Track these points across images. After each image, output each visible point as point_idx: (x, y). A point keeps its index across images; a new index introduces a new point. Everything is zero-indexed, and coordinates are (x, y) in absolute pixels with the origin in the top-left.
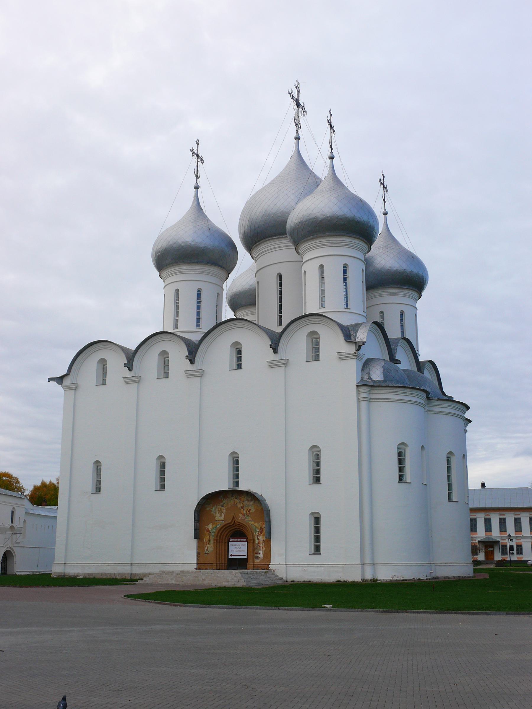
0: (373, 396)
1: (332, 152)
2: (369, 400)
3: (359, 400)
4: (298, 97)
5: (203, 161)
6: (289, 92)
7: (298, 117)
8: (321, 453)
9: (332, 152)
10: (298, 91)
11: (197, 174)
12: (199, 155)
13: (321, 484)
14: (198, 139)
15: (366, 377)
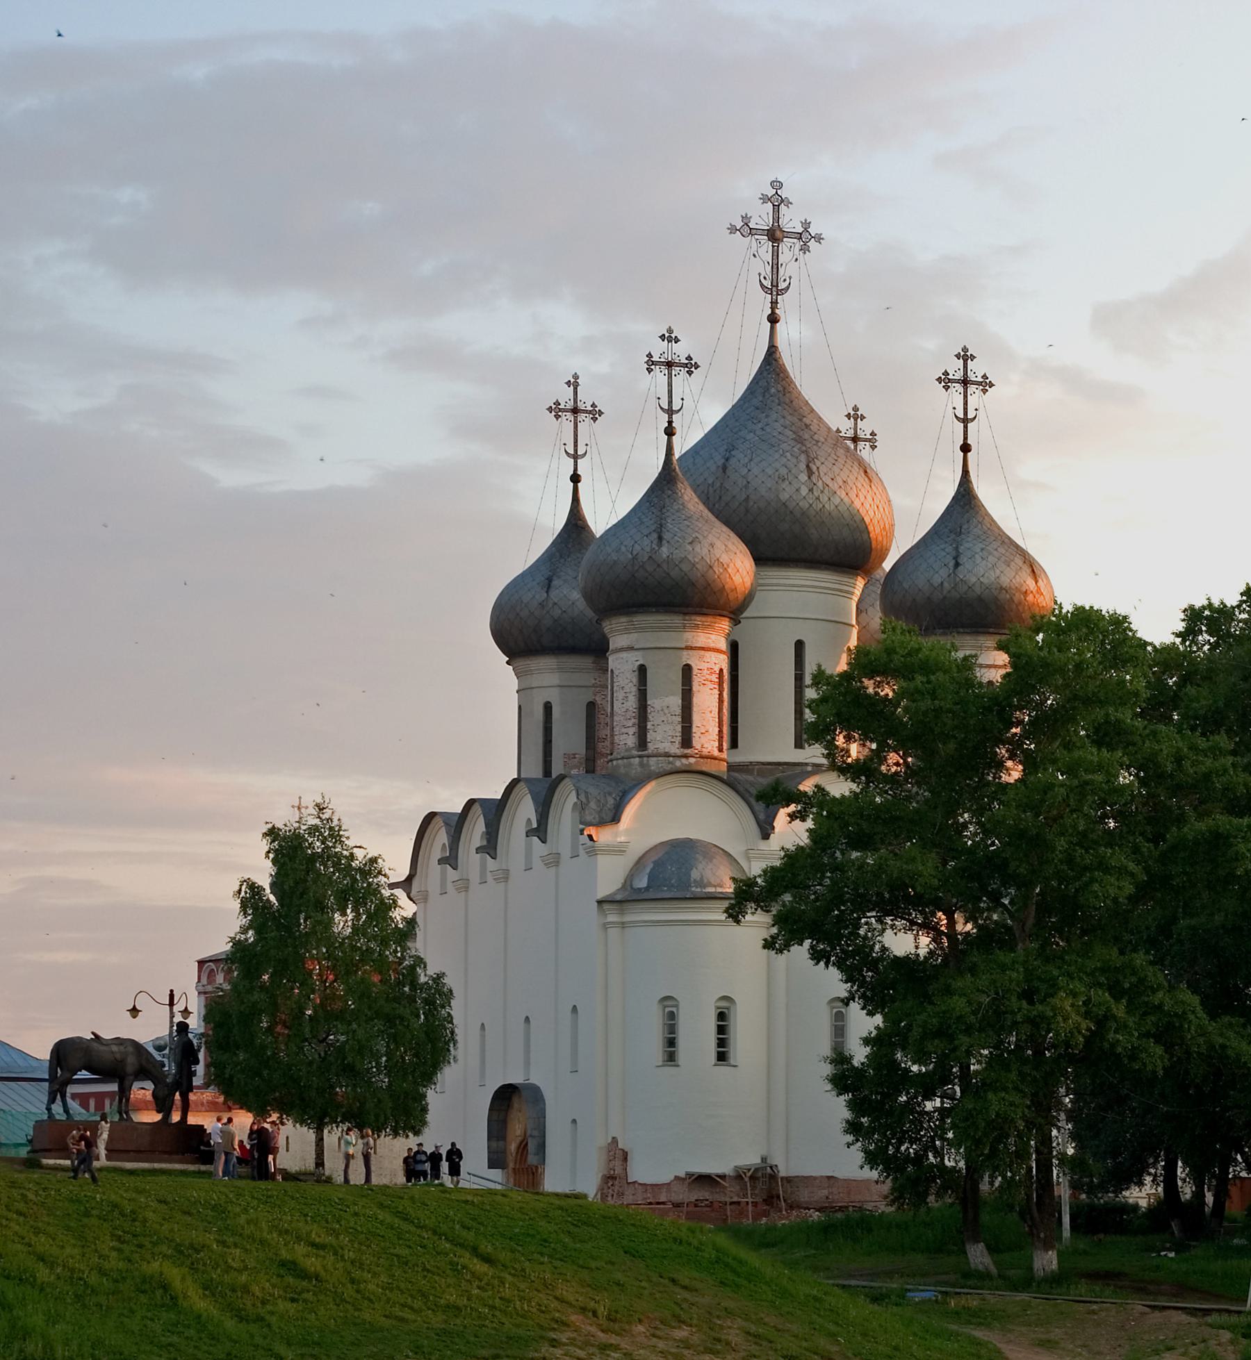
0: (627, 918)
1: (670, 423)
2: (623, 925)
3: (605, 926)
4: (777, 218)
5: (595, 413)
6: (733, 229)
7: (775, 266)
8: (680, 1010)
9: (670, 423)
10: (777, 202)
11: (576, 451)
12: (581, 406)
13: (678, 1066)
14: (576, 377)
15: (628, 883)
